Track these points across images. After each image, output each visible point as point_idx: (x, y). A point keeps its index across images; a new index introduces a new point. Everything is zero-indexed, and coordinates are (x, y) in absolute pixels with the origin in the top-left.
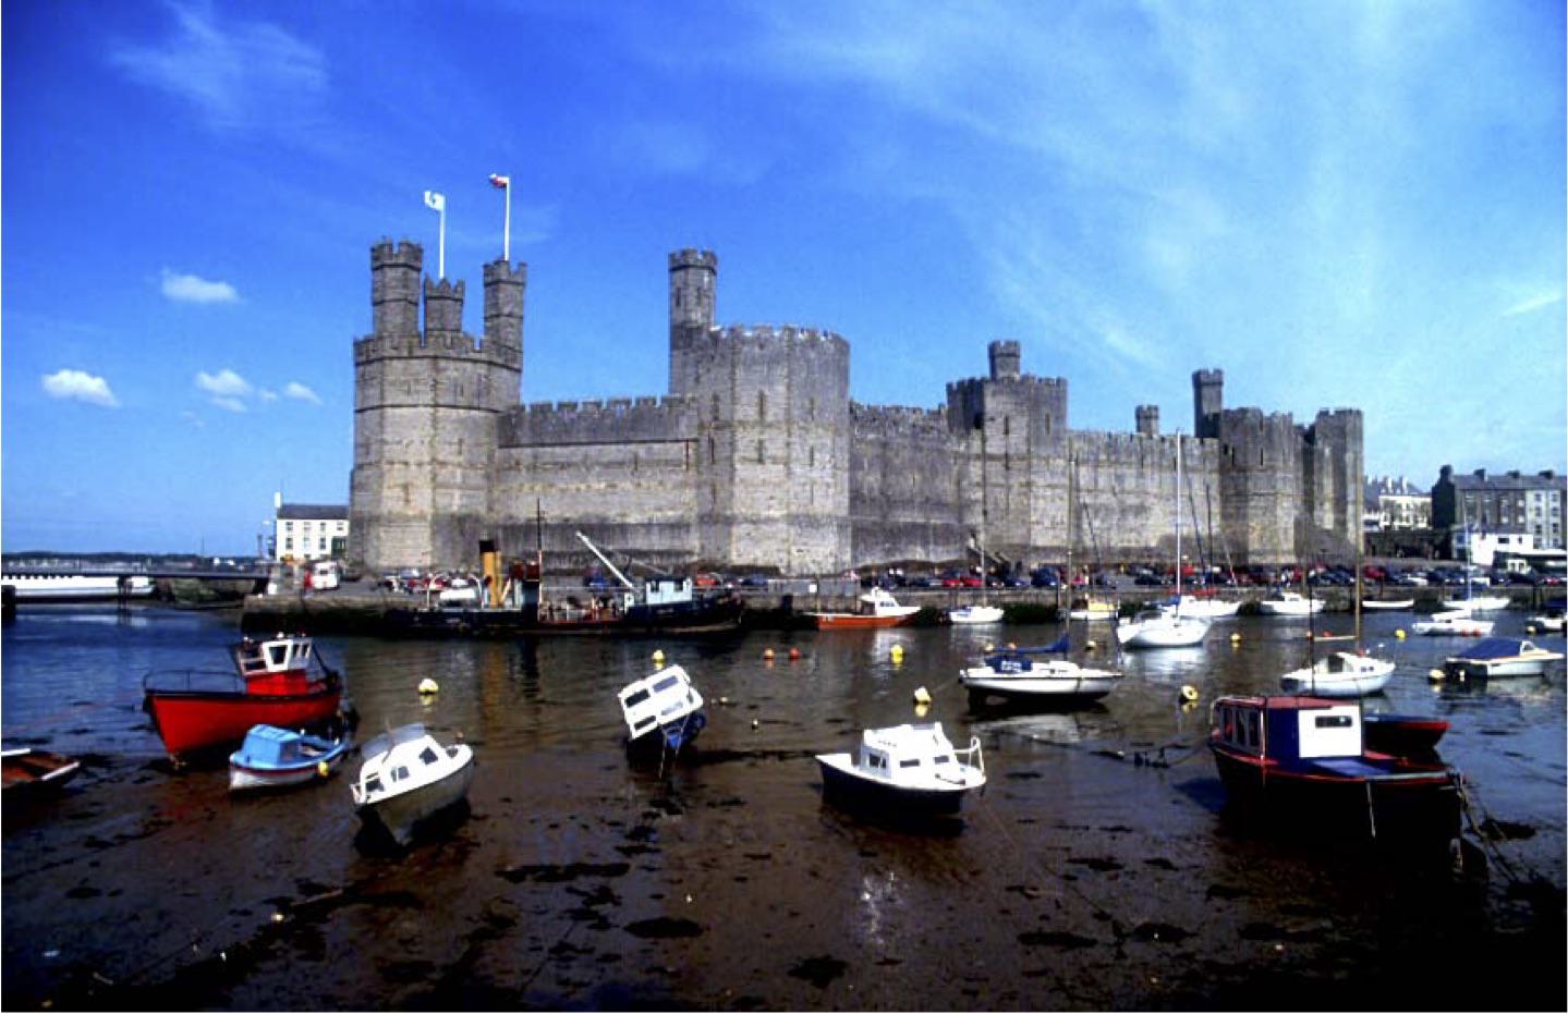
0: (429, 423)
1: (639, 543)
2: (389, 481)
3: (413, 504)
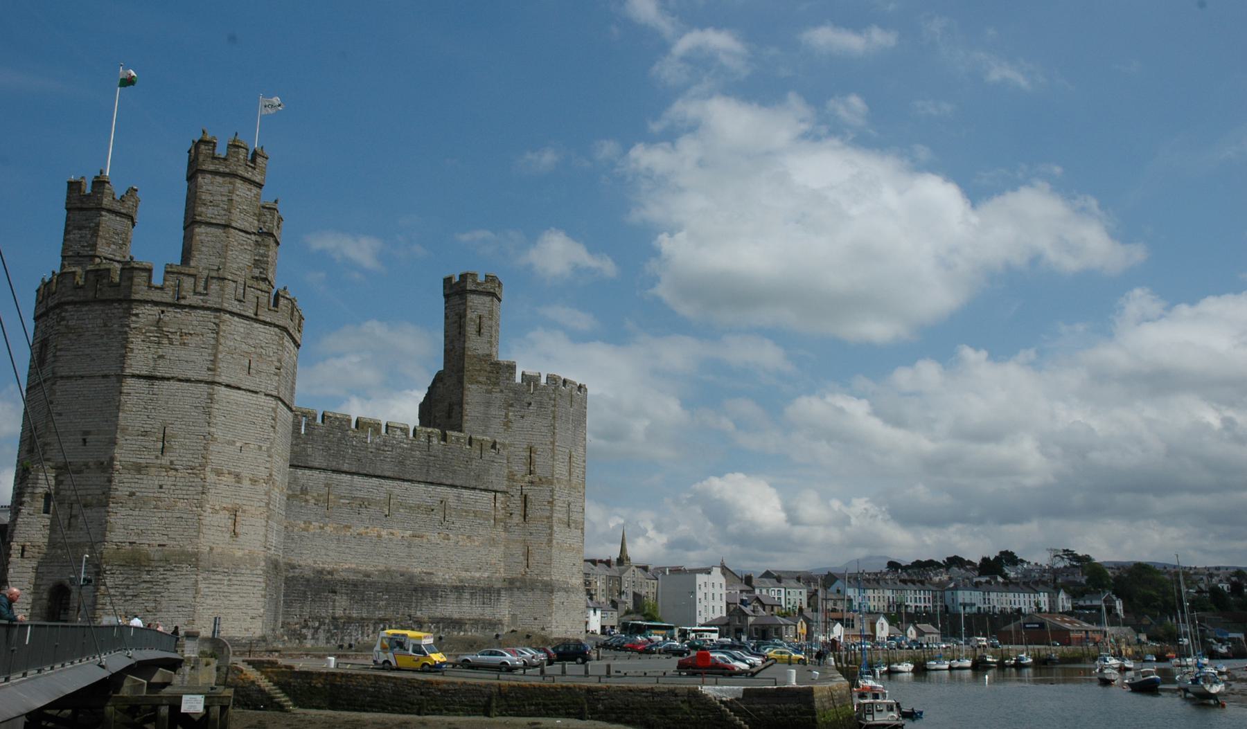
0: (269, 421)
1: (450, 609)
2: (212, 500)
3: (241, 538)
